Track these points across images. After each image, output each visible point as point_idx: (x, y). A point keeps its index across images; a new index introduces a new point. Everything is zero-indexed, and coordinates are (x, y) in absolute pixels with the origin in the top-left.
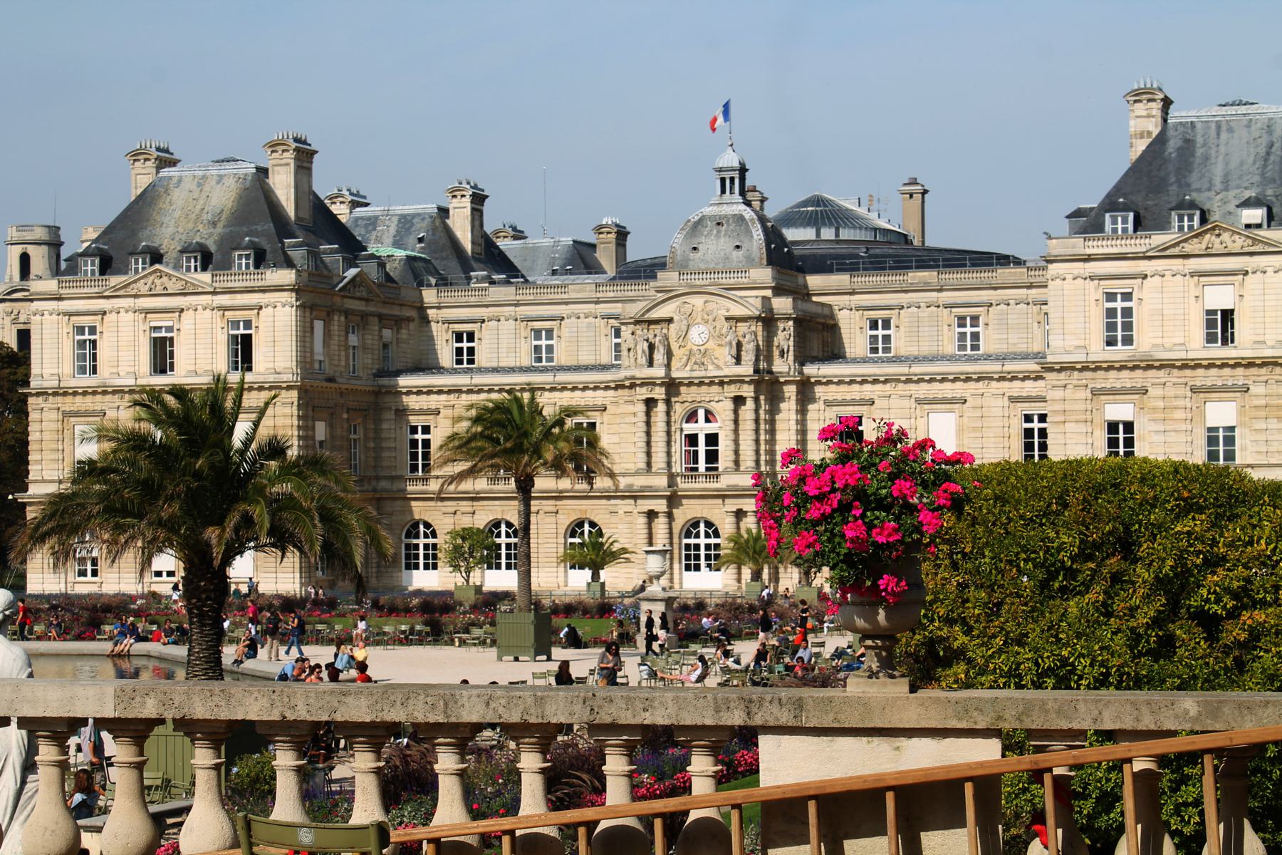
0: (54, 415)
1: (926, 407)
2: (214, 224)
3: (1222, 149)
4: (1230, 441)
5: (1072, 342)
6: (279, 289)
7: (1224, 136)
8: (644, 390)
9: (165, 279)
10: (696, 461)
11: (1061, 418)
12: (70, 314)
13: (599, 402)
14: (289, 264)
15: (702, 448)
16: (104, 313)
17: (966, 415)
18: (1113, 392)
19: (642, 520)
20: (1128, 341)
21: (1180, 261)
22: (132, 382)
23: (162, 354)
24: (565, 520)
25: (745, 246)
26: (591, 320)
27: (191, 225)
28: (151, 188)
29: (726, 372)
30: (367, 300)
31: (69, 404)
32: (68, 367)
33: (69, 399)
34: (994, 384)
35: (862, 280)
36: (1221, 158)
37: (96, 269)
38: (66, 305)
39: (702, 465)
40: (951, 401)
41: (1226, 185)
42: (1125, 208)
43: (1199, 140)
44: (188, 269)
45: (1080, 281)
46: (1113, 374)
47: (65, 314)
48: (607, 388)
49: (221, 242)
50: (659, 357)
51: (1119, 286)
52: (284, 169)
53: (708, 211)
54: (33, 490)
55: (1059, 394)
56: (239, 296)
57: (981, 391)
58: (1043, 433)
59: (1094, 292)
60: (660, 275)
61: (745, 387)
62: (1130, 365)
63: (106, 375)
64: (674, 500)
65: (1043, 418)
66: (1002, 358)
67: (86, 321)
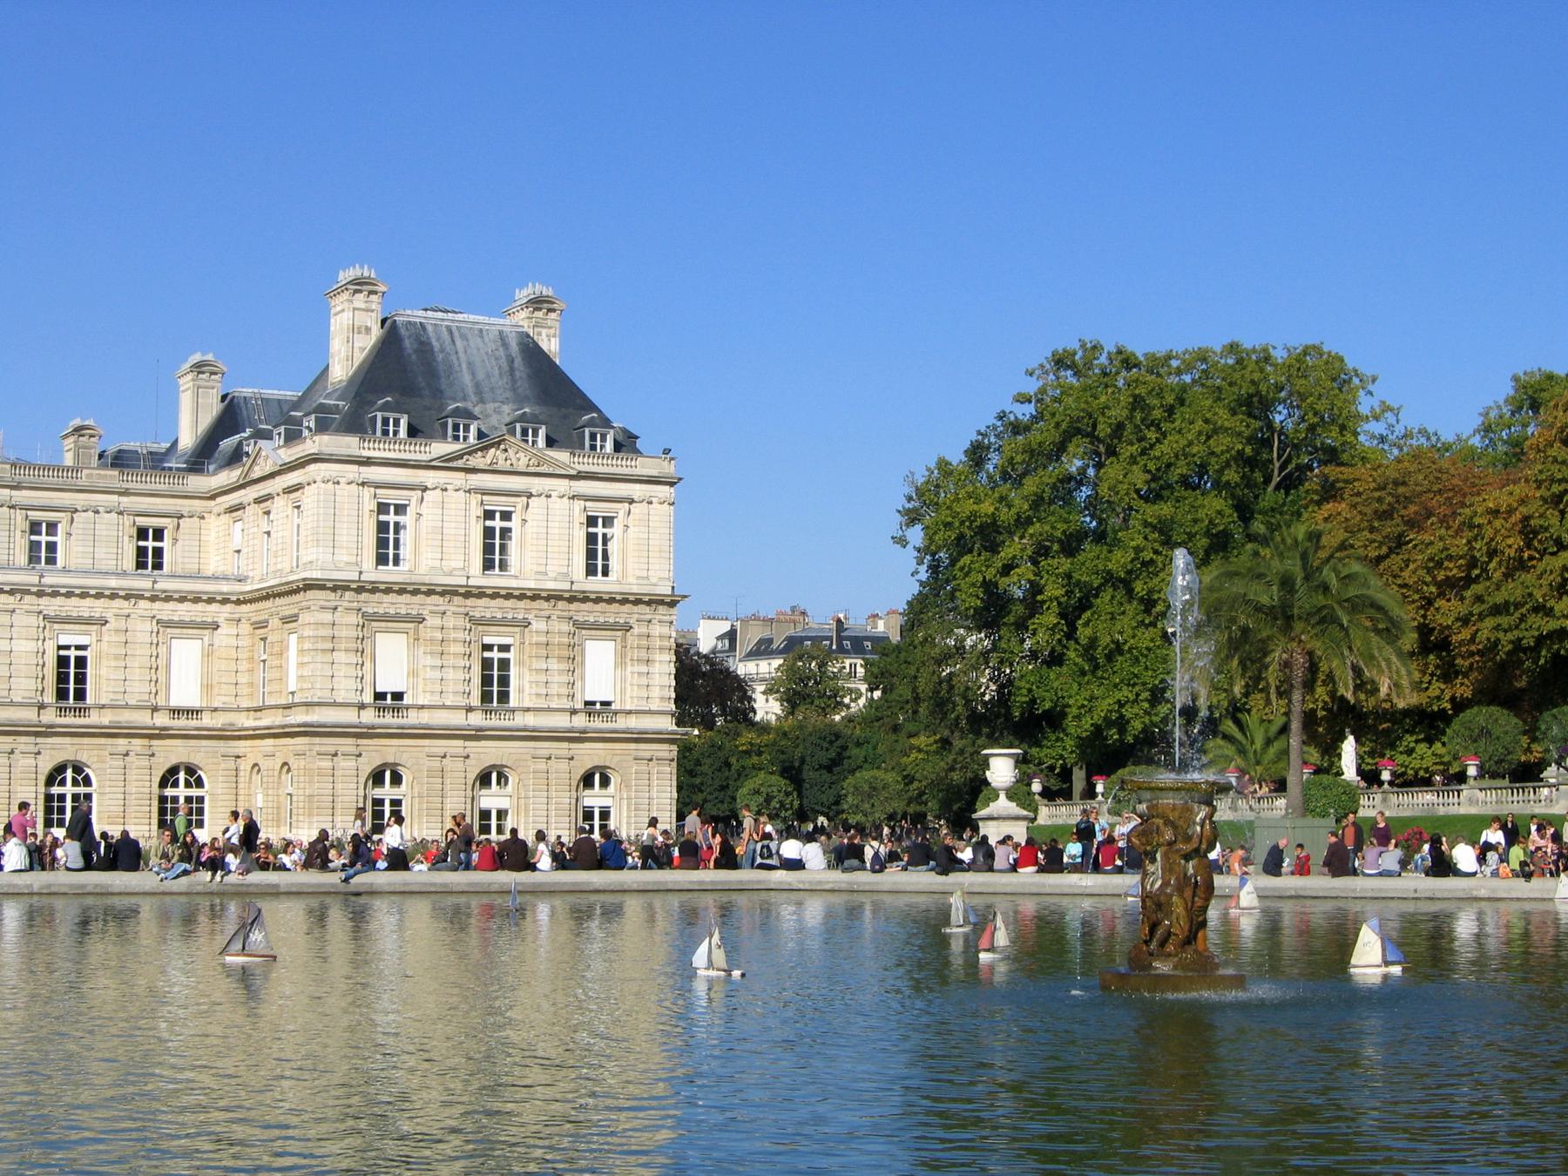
1: (56, 626)
3: (461, 355)
4: (504, 681)
5: (344, 557)
7: (459, 343)
11: (330, 646)
17: (105, 638)
18: (386, 618)
21: (462, 475)
34: (143, 604)
36: (464, 366)
40: (88, 621)
43: (435, 344)
45: (354, 486)
51: (392, 497)
55: (327, 617)
57: (126, 612)
62: (410, 588)
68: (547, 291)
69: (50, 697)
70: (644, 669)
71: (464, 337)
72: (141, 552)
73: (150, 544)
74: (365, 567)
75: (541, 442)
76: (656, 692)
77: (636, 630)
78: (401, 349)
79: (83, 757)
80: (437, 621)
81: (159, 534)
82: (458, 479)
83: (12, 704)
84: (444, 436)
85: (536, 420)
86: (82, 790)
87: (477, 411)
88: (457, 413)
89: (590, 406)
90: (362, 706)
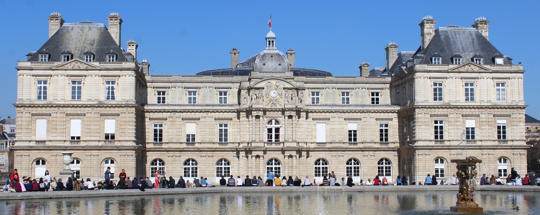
0: (28, 115)
2: (92, 45)
3: (459, 40)
4: (473, 132)
7: (458, 36)
8: (255, 112)
9: (79, 64)
10: (271, 138)
12: (37, 76)
13: (230, 117)
15: (274, 134)
16: (51, 76)
19: (254, 158)
20: (441, 99)
22: (63, 103)
23: (76, 93)
24: (216, 159)
25: (283, 64)
26: (211, 89)
27: (82, 45)
29: (286, 107)
30: (141, 77)
33: (35, 109)
37: (47, 58)
38: (34, 72)
39: (273, 139)
42: (439, 56)
43: (450, 36)
44: (87, 60)
45: (426, 79)
46: (437, 110)
47: (33, 76)
48: (234, 112)
49: (97, 51)
51: (438, 81)
52: (116, 26)
53: (265, 51)
54: (16, 144)
55: (420, 116)
56: (110, 71)
58: (386, 131)
59: (430, 83)
60: (252, 73)
61: (293, 112)
63: (52, 100)
64: (265, 152)
65: (386, 126)
68: (484, 19)
70: (515, 127)
71: (459, 34)
72: (373, 99)
73: (375, 97)
74: (430, 101)
75: (482, 63)
78: (440, 39)
80: (451, 116)
81: (377, 94)
83: (337, 143)
85: (480, 56)
86: (356, 166)
87: (462, 55)
88: (456, 56)
89: (496, 51)
90: (431, 141)
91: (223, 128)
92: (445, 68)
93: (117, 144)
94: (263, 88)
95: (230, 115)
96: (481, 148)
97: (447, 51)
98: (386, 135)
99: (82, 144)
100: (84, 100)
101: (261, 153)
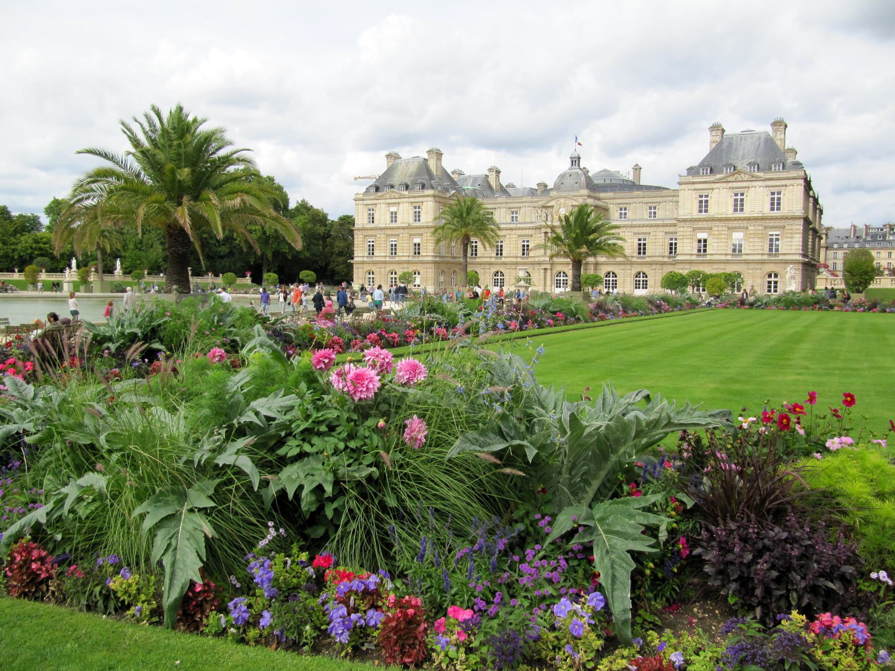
6: (428, 196)
14: (432, 188)
20: (706, 211)
23: (394, 216)
28: (393, 165)
31: (366, 233)
32: (366, 221)
35: (617, 195)
38: (365, 202)
40: (645, 233)
41: (743, 158)
49: (412, 182)
50: (549, 218)
51: (704, 193)
54: (355, 259)
55: (682, 229)
59: (695, 195)
66: (663, 220)
67: (371, 207)
69: (636, 254)
76: (794, 247)
77: (787, 227)
79: (644, 270)
82: (724, 185)
84: (721, 172)
88: (728, 165)
90: (691, 255)
91: (526, 244)
92: (711, 178)
93: (421, 259)
94: (553, 206)
95: (530, 232)
96: (747, 262)
97: (725, 159)
98: (676, 248)
99: (397, 259)
100: (398, 224)
101: (549, 267)
